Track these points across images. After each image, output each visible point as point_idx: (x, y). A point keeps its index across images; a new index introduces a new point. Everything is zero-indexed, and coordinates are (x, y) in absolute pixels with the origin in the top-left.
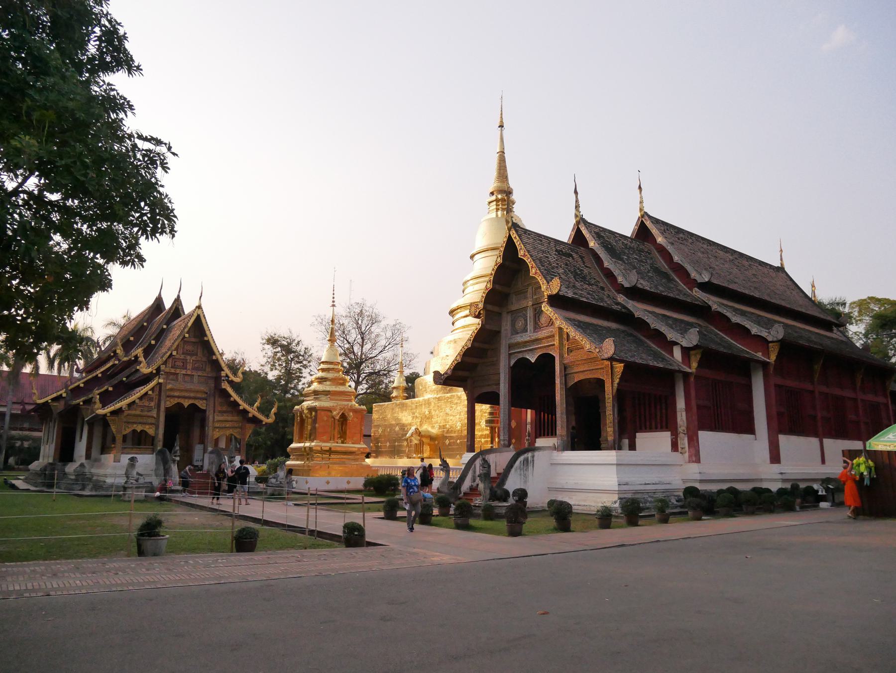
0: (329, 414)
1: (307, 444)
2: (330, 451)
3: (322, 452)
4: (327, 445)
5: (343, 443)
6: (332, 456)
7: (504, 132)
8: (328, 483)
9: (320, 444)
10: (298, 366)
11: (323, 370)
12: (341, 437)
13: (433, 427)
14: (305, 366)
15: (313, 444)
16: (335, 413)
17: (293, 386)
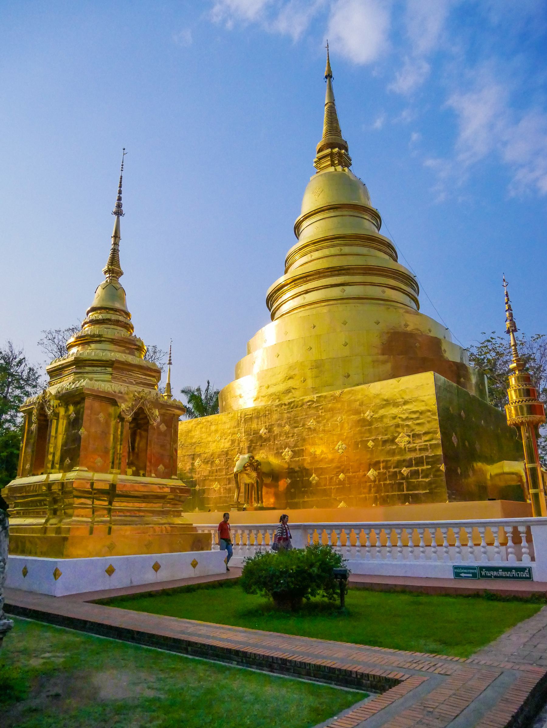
0: (111, 410)
1: (56, 476)
2: (112, 492)
3: (94, 493)
4: (104, 478)
5: (136, 474)
6: (117, 505)
7: (333, 83)
8: (110, 571)
9: (89, 475)
10: (18, 392)
11: (93, 322)
12: (130, 464)
13: (278, 454)
14: (28, 394)
15: (71, 475)
16: (123, 406)
17: (8, 417)
